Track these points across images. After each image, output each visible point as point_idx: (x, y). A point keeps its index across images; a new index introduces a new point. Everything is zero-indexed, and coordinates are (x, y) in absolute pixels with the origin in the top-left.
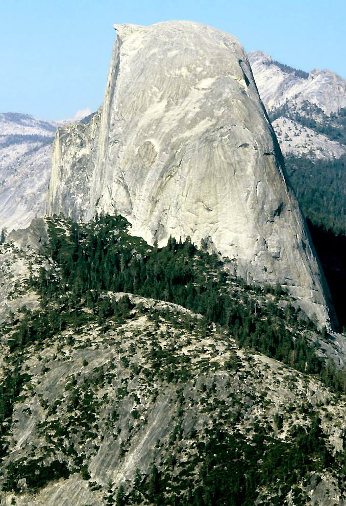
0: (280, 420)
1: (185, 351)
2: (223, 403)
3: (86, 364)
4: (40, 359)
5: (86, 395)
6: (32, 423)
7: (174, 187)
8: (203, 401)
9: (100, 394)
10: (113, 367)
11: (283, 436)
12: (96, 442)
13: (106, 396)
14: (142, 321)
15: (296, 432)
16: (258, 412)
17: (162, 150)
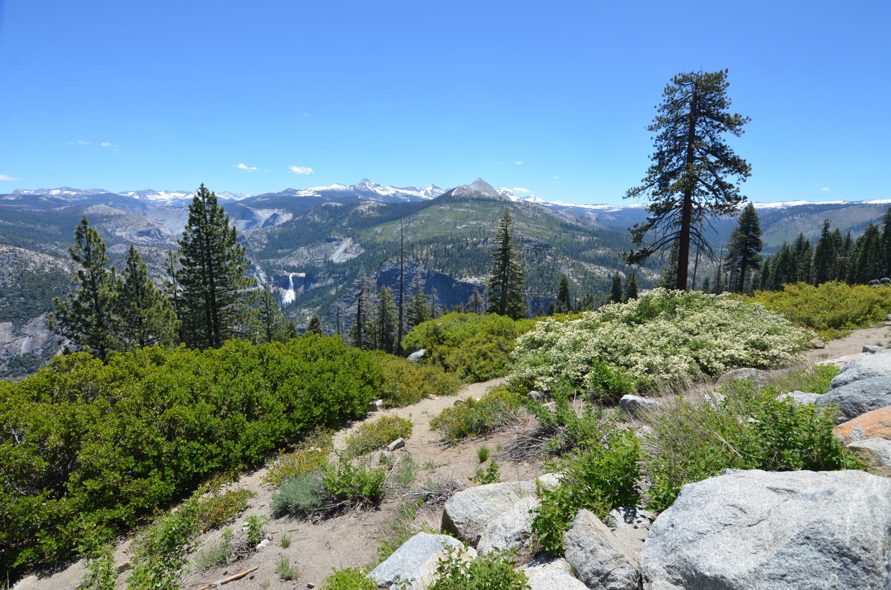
0: (43, 267)
2: (16, 263)
8: (7, 263)
15: (52, 270)
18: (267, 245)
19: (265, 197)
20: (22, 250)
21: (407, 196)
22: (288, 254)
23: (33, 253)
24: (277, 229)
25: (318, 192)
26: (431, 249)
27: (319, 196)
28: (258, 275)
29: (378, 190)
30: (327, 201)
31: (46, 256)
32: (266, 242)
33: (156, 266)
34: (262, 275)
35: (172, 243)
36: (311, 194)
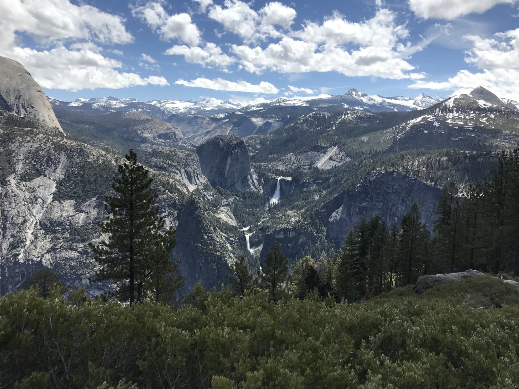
1: (61, 143)
2: (82, 155)
3: (31, 147)
4: (15, 146)
5: (36, 155)
6: (21, 163)
7: (21, 102)
9: (41, 154)
10: (42, 147)
11: (101, 162)
12: (45, 167)
13: (43, 155)
14: (41, 135)
15: (104, 162)
16: (92, 157)
17: (14, 91)
18: (259, 150)
19: (260, 107)
20: (86, 145)
21: (394, 105)
22: (277, 159)
23: (92, 148)
24: (269, 136)
25: (307, 102)
26: (423, 160)
27: (308, 105)
28: (251, 176)
29: (364, 99)
30: (315, 111)
31: (100, 150)
32: (259, 147)
33: (174, 164)
34: (255, 176)
35: (184, 144)
36: (300, 104)
